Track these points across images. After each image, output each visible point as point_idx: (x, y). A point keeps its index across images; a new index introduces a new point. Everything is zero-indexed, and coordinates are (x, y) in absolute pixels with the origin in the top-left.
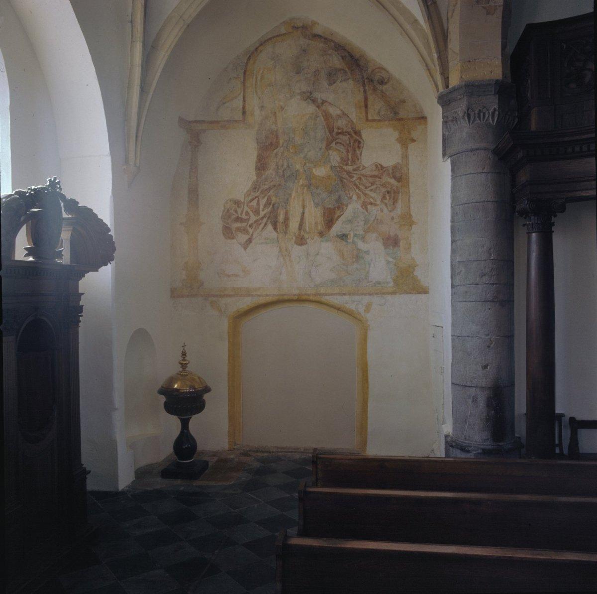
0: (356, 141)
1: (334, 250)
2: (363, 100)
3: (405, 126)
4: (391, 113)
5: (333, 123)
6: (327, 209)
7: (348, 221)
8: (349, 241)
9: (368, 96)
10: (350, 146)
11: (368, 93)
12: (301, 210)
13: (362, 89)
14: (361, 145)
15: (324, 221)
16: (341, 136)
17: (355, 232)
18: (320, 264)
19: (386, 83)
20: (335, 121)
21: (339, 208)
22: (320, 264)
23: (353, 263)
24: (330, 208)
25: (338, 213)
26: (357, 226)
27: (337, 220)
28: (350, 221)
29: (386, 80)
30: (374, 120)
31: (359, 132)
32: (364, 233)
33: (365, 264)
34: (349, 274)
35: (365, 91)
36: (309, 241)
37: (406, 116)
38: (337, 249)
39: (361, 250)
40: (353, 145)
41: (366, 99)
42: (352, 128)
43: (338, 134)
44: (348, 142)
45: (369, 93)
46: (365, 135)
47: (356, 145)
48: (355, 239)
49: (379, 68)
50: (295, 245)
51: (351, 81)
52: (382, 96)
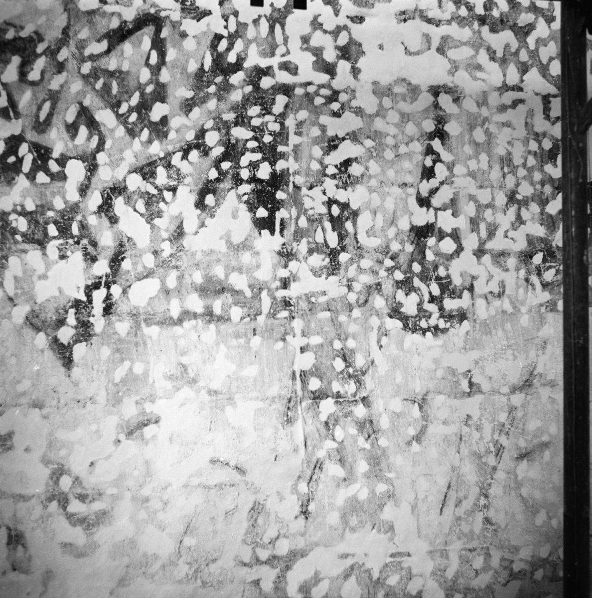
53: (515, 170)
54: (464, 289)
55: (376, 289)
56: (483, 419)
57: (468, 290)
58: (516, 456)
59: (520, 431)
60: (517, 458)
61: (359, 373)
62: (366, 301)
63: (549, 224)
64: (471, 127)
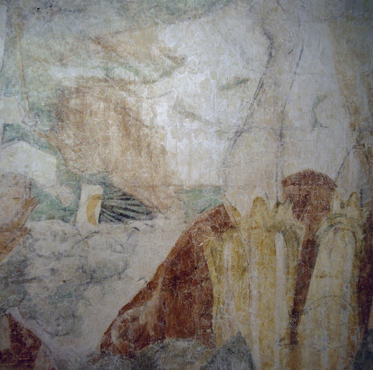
1: (163, 151)
6: (192, 334)
7: (99, 282)
8: (98, 190)
12: (306, 323)
15: (208, 279)
17: (68, 228)
18: (227, 87)
21: (142, 338)
22: (227, 87)
23: (78, 90)
24: (181, 335)
25: (146, 314)
26: (58, 257)
27: (151, 286)
28: (92, 276)
32: (29, 225)
33: (24, 85)
34: (97, 41)
36: (277, 192)
38: (150, 155)
39: (41, 147)
48: (66, 195)
50: (332, 176)
53: (241, 291)
54: (284, 204)
55: (344, 204)
56: (273, 111)
57: (281, 203)
58: (249, 82)
59: (245, 100)
60: (247, 80)
61: (357, 147)
62: (351, 196)
63: (216, 252)
64: (272, 321)
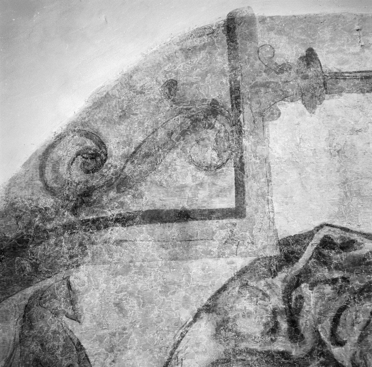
0: (320, 257)
2: (158, 228)
3: (259, 80)
4: (211, 126)
5: (251, 352)
9: (145, 209)
10: (344, 279)
11: (134, 208)
13: (117, 232)
14: (336, 235)
16: (305, 321)
19: (101, 144)
20: (243, 346)
29: (89, 143)
30: (239, 187)
31: (284, 243)
35: (124, 220)
37: (225, 80)
40: (337, 268)
41: (155, 217)
42: (274, 274)
43: (295, 333)
44: (328, 289)
45: (133, 206)
46: (291, 225)
47: (336, 257)
49: (42, 168)
51: (80, 277)
52: (147, 155)
